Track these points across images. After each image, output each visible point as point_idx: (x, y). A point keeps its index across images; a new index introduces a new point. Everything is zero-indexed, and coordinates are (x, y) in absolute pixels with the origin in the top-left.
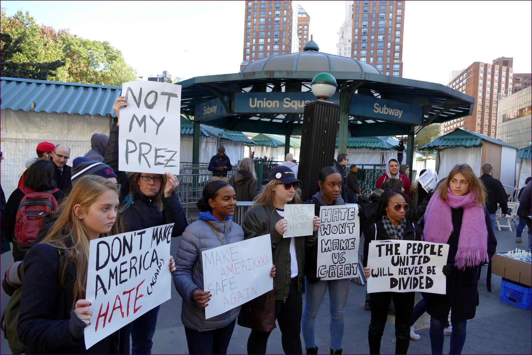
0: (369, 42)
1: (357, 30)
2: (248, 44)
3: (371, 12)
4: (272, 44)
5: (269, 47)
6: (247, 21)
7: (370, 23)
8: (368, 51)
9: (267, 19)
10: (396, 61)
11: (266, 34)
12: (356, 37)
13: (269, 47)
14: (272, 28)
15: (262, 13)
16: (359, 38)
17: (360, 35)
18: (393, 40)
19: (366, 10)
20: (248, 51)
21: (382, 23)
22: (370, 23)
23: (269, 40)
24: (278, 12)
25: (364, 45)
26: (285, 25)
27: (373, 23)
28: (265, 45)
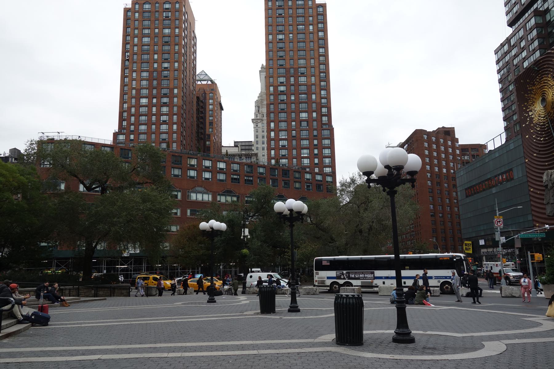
0: (288, 103)
1: (272, 89)
2: (126, 106)
3: (288, 66)
4: (160, 105)
5: (154, 109)
6: (123, 77)
7: (288, 80)
8: (289, 115)
9: (151, 73)
10: (324, 127)
11: (151, 92)
12: (272, 97)
13: (154, 109)
14: (159, 84)
15: (145, 65)
16: (276, 98)
17: (277, 93)
18: (318, 101)
19: (281, 64)
20: (125, 114)
21: (302, 79)
22: (288, 80)
23: (155, 101)
24: (166, 65)
25: (283, 106)
26: (176, 81)
27: (292, 79)
28: (150, 106)
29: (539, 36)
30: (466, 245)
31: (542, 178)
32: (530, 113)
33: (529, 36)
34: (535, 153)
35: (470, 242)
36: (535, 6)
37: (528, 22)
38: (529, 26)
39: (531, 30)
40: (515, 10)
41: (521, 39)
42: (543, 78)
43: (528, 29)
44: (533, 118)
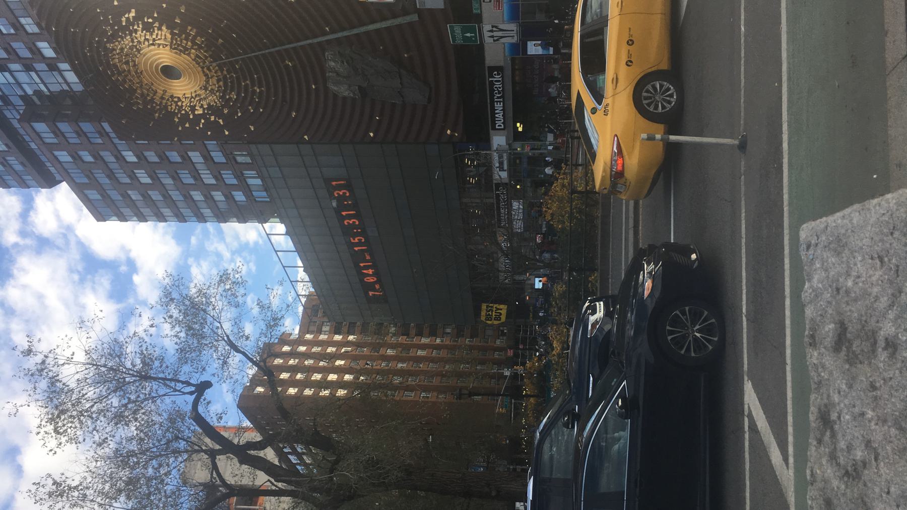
29: (74, 120)
30: (489, 317)
31: (345, 98)
32: (200, 111)
33: (71, 141)
34: (289, 114)
35: (484, 306)
36: (16, 125)
37: (41, 138)
38: (49, 138)
39: (57, 133)
40: (18, 167)
41: (76, 158)
42: (115, 65)
43: (55, 141)
44: (209, 105)
